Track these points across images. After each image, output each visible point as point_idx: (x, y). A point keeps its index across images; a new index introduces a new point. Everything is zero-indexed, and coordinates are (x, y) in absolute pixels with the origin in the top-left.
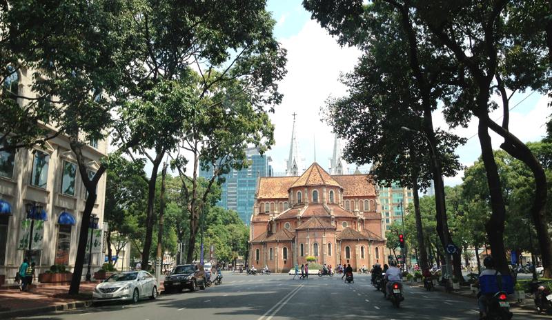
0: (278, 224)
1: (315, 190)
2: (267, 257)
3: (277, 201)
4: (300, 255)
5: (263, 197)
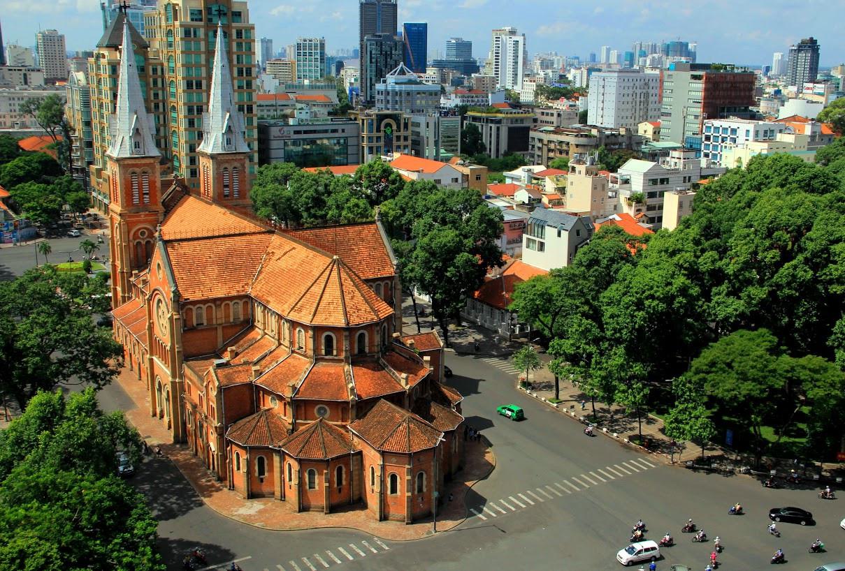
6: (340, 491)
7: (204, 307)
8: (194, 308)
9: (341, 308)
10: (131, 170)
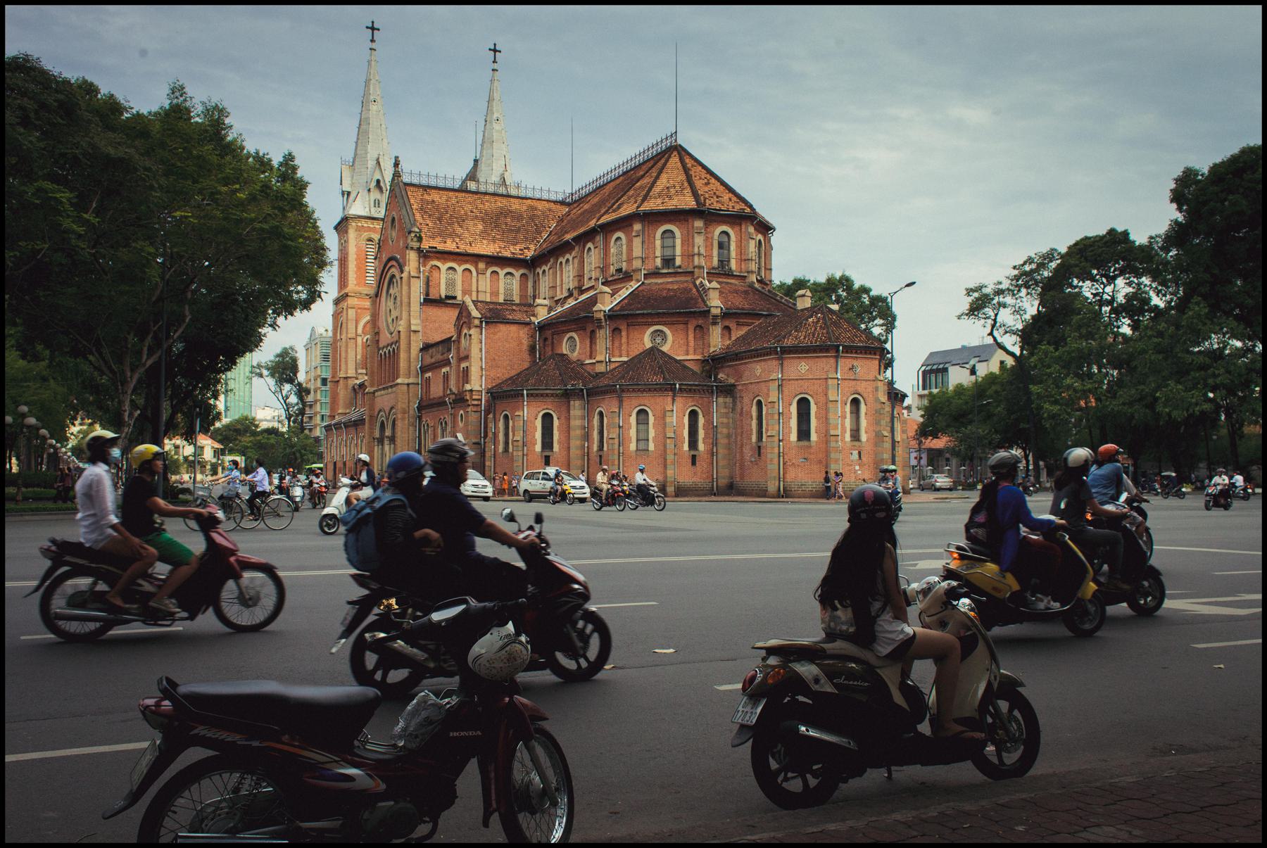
1: (725, 228)
3: (482, 265)
4: (794, 437)
5: (440, 247)
6: (694, 457)
7: (460, 269)
8: (444, 267)
9: (689, 190)
10: (366, 235)
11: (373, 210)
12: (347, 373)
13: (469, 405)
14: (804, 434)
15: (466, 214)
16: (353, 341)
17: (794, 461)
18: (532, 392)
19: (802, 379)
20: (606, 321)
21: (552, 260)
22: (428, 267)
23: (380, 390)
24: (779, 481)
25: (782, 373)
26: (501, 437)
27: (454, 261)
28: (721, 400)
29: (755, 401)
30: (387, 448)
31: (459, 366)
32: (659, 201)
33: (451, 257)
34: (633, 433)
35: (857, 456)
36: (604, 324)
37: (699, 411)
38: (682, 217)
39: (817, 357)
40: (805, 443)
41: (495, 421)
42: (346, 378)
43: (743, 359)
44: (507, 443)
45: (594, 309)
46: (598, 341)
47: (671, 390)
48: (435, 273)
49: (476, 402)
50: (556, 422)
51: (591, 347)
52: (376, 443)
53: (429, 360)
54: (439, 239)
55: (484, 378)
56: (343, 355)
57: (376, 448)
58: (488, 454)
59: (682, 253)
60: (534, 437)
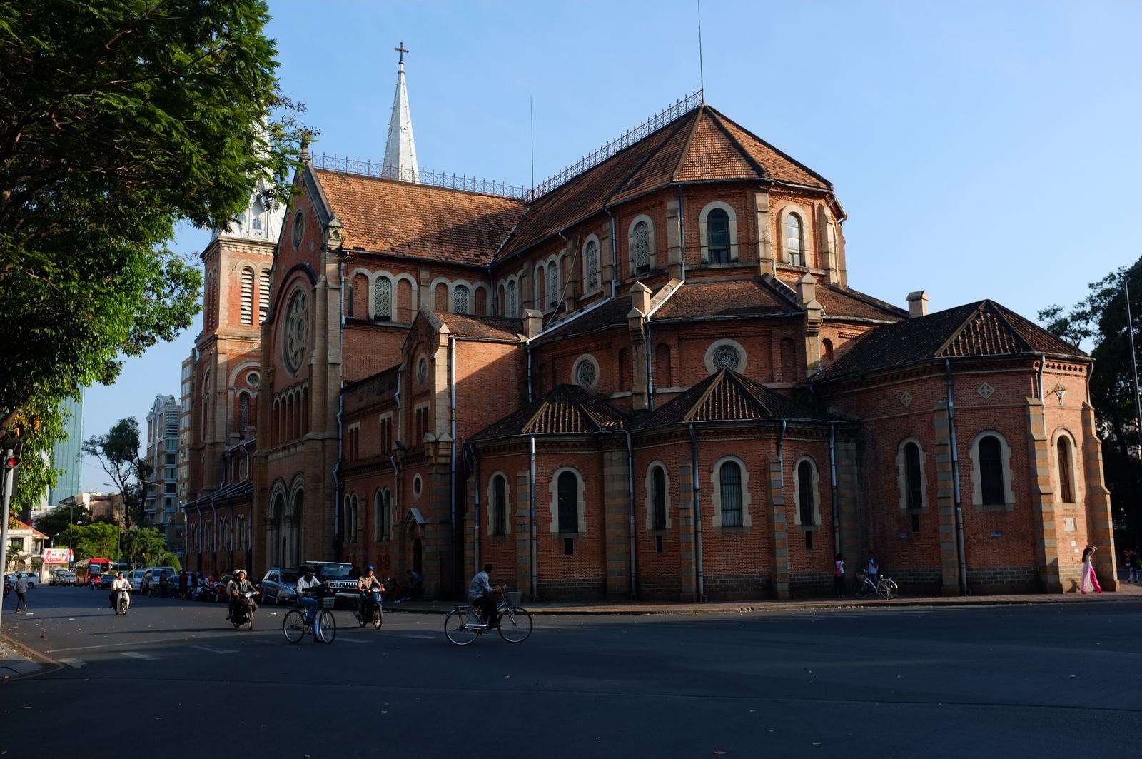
0: (662, 350)
2: (704, 512)
3: (424, 275)
4: (977, 499)
5: (370, 249)
6: (809, 534)
7: (395, 279)
8: (373, 276)
11: (252, 232)
12: (214, 437)
13: (432, 465)
14: (993, 491)
15: (399, 208)
16: (222, 395)
17: (980, 537)
18: (543, 440)
19: (986, 409)
20: (646, 334)
21: (526, 265)
22: (351, 276)
23: (276, 451)
24: (960, 568)
25: (953, 400)
26: (490, 511)
27: (386, 268)
28: (841, 445)
29: (902, 446)
30: (286, 532)
31: (411, 408)
32: (701, 170)
33: (384, 263)
34: (716, 499)
35: (1072, 525)
36: (644, 337)
37: (813, 465)
38: (737, 191)
39: (1007, 374)
40: (998, 508)
41: (481, 486)
42: (213, 444)
43: (874, 383)
44: (500, 520)
45: (628, 316)
46: (634, 363)
47: (775, 431)
48: (361, 285)
49: (443, 460)
50: (581, 487)
51: (621, 374)
52: (269, 527)
53: (354, 404)
54: (365, 238)
55: (454, 423)
56: (210, 414)
57: (269, 533)
58: (469, 539)
59: (739, 241)
60: (547, 509)
